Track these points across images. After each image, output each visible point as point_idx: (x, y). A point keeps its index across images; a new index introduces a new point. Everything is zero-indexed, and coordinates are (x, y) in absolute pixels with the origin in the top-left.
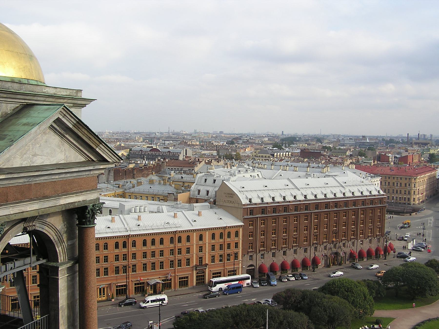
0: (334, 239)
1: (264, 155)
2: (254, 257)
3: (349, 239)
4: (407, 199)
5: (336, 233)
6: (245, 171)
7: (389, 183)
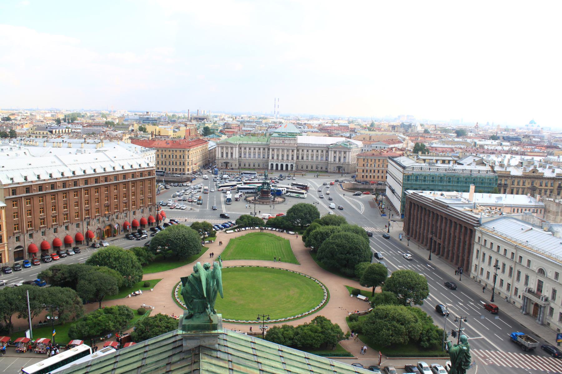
0: (107, 213)
2: (22, 238)
3: (121, 211)
4: (182, 170)
5: (108, 207)
6: (9, 149)
7: (165, 155)
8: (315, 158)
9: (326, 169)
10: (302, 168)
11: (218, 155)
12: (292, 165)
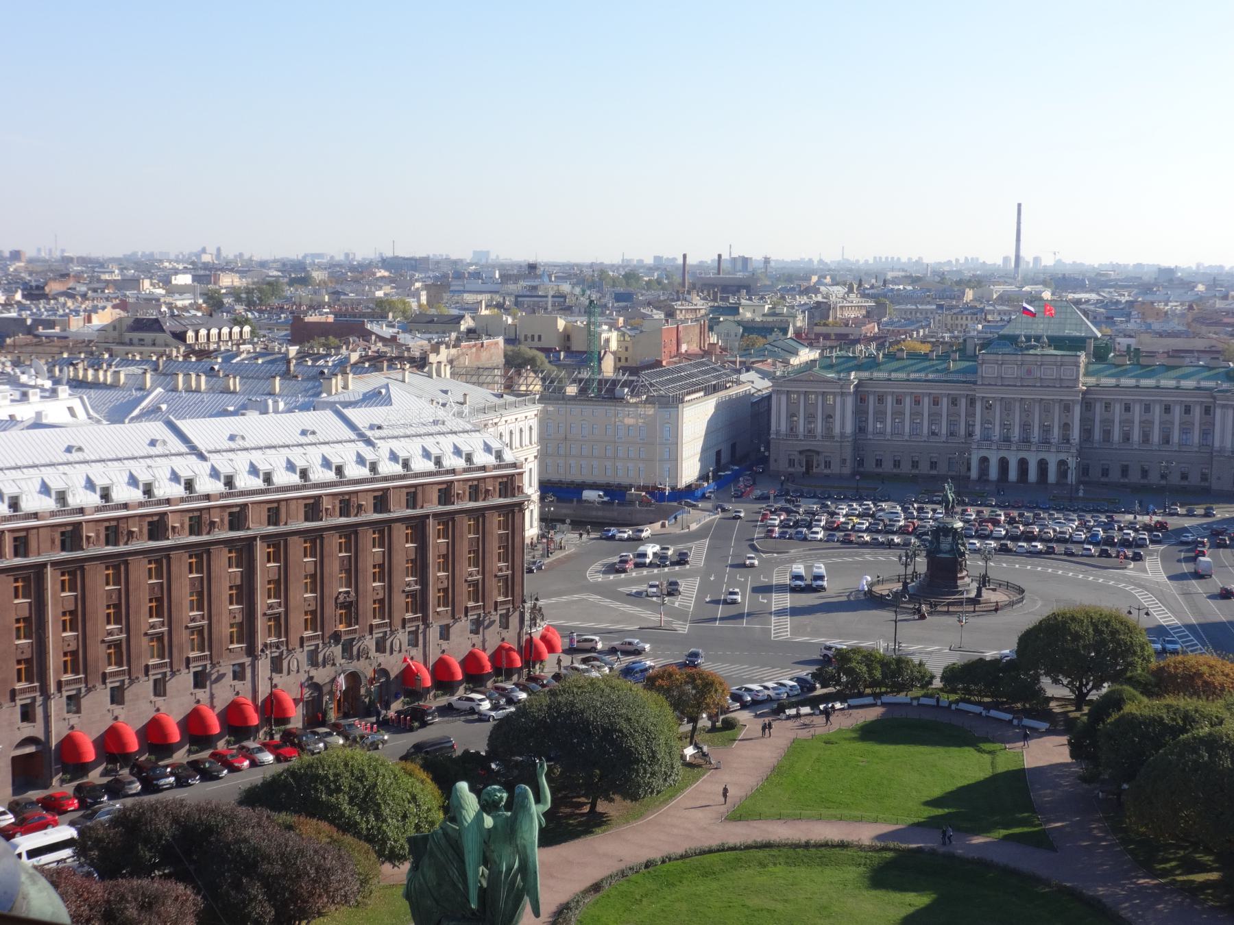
0: (342, 628)
1: (148, 336)
6: (17, 395)
8: (1156, 437)
9: (1204, 477)
10: (1105, 472)
11: (779, 423)
12: (1062, 463)
